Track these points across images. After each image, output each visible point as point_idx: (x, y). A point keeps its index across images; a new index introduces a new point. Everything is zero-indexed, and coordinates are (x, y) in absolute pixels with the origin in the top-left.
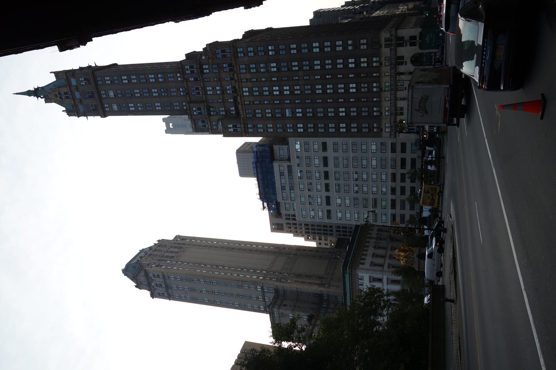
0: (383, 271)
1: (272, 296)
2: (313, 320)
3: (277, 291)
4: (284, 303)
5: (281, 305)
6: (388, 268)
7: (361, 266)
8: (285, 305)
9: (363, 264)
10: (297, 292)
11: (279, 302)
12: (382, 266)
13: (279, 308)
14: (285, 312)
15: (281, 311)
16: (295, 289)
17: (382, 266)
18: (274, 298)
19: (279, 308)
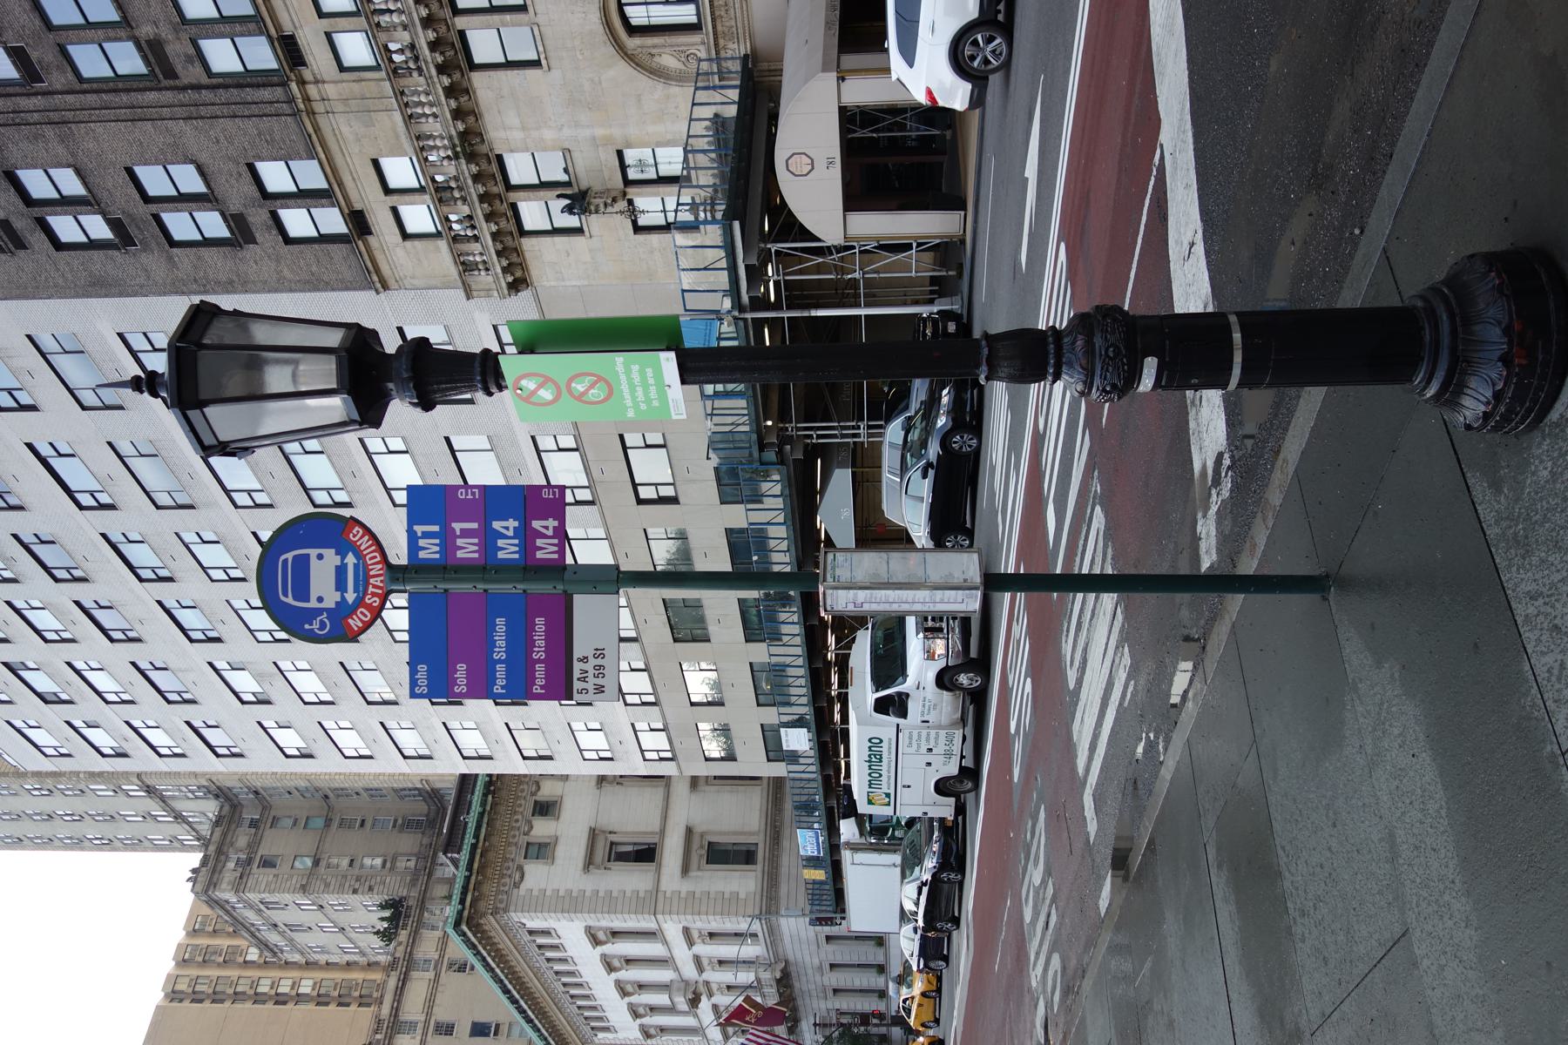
0: (652, 902)
1: (211, 808)
2: (403, 935)
3: (220, 792)
4: (264, 850)
5: (249, 861)
6: (685, 870)
7: (536, 876)
8: (267, 863)
9: (542, 851)
10: (317, 790)
11: (242, 842)
12: (646, 854)
13: (239, 886)
14: (268, 897)
15: (253, 897)
16: (302, 784)
17: (646, 854)
18: (217, 822)
19: (239, 886)
